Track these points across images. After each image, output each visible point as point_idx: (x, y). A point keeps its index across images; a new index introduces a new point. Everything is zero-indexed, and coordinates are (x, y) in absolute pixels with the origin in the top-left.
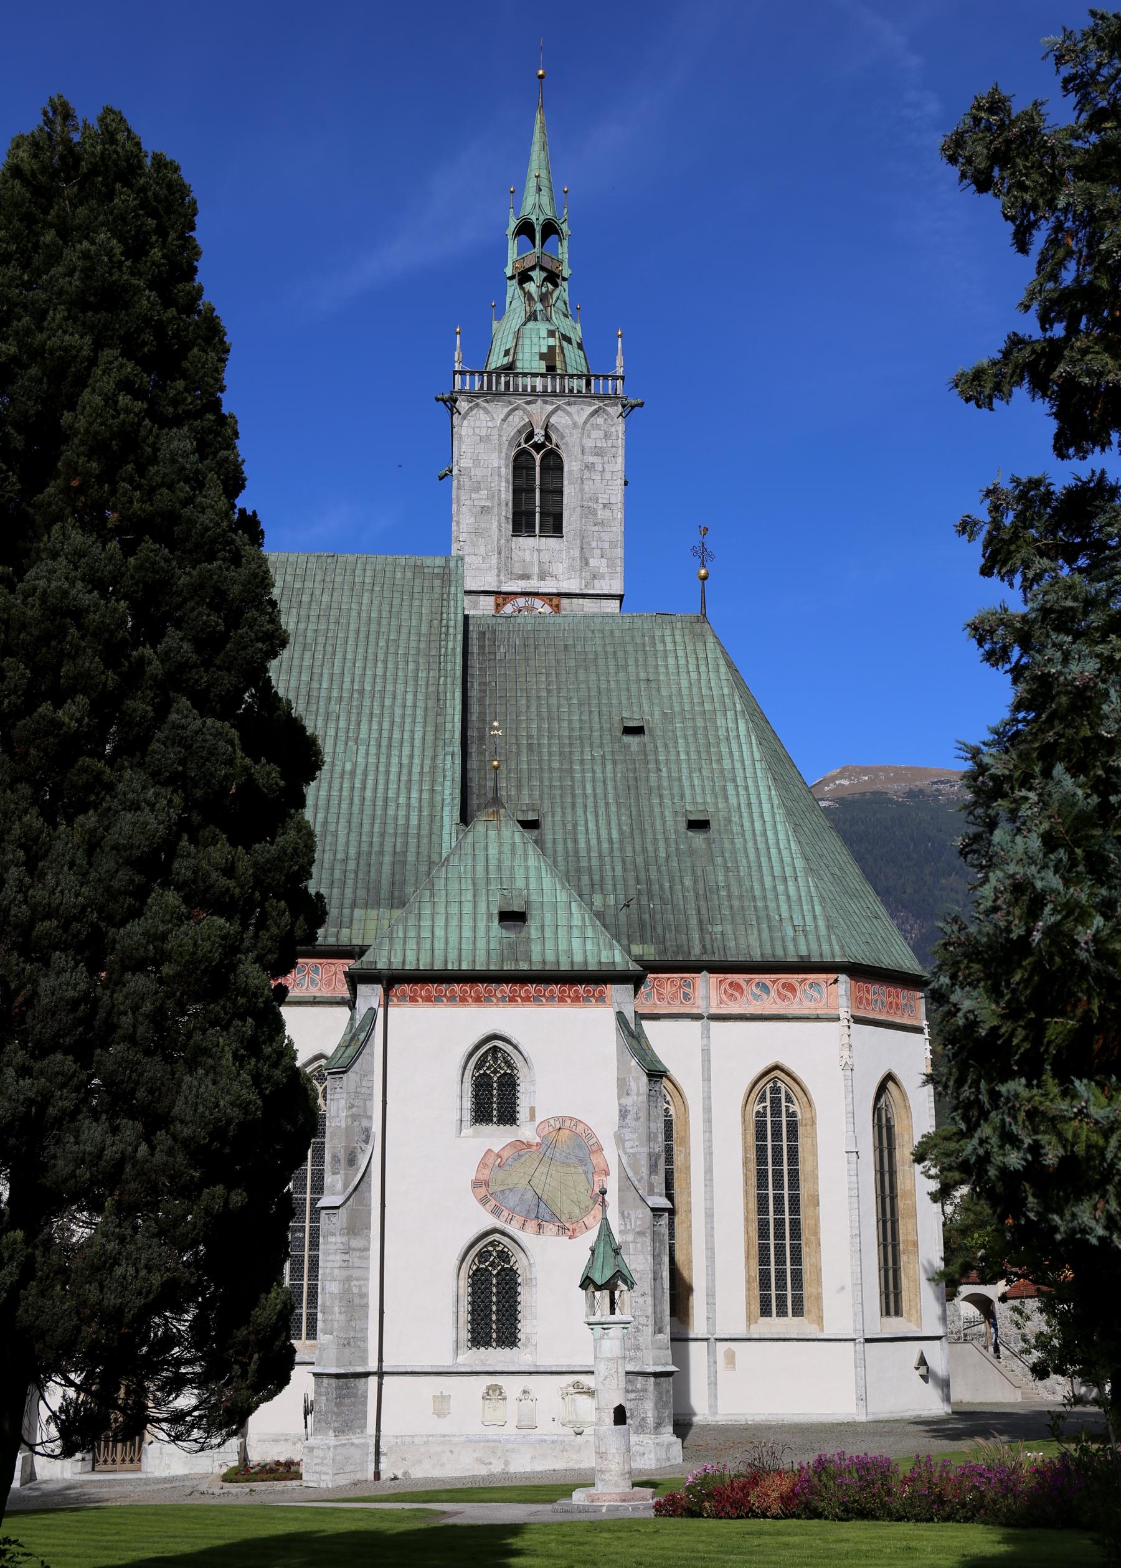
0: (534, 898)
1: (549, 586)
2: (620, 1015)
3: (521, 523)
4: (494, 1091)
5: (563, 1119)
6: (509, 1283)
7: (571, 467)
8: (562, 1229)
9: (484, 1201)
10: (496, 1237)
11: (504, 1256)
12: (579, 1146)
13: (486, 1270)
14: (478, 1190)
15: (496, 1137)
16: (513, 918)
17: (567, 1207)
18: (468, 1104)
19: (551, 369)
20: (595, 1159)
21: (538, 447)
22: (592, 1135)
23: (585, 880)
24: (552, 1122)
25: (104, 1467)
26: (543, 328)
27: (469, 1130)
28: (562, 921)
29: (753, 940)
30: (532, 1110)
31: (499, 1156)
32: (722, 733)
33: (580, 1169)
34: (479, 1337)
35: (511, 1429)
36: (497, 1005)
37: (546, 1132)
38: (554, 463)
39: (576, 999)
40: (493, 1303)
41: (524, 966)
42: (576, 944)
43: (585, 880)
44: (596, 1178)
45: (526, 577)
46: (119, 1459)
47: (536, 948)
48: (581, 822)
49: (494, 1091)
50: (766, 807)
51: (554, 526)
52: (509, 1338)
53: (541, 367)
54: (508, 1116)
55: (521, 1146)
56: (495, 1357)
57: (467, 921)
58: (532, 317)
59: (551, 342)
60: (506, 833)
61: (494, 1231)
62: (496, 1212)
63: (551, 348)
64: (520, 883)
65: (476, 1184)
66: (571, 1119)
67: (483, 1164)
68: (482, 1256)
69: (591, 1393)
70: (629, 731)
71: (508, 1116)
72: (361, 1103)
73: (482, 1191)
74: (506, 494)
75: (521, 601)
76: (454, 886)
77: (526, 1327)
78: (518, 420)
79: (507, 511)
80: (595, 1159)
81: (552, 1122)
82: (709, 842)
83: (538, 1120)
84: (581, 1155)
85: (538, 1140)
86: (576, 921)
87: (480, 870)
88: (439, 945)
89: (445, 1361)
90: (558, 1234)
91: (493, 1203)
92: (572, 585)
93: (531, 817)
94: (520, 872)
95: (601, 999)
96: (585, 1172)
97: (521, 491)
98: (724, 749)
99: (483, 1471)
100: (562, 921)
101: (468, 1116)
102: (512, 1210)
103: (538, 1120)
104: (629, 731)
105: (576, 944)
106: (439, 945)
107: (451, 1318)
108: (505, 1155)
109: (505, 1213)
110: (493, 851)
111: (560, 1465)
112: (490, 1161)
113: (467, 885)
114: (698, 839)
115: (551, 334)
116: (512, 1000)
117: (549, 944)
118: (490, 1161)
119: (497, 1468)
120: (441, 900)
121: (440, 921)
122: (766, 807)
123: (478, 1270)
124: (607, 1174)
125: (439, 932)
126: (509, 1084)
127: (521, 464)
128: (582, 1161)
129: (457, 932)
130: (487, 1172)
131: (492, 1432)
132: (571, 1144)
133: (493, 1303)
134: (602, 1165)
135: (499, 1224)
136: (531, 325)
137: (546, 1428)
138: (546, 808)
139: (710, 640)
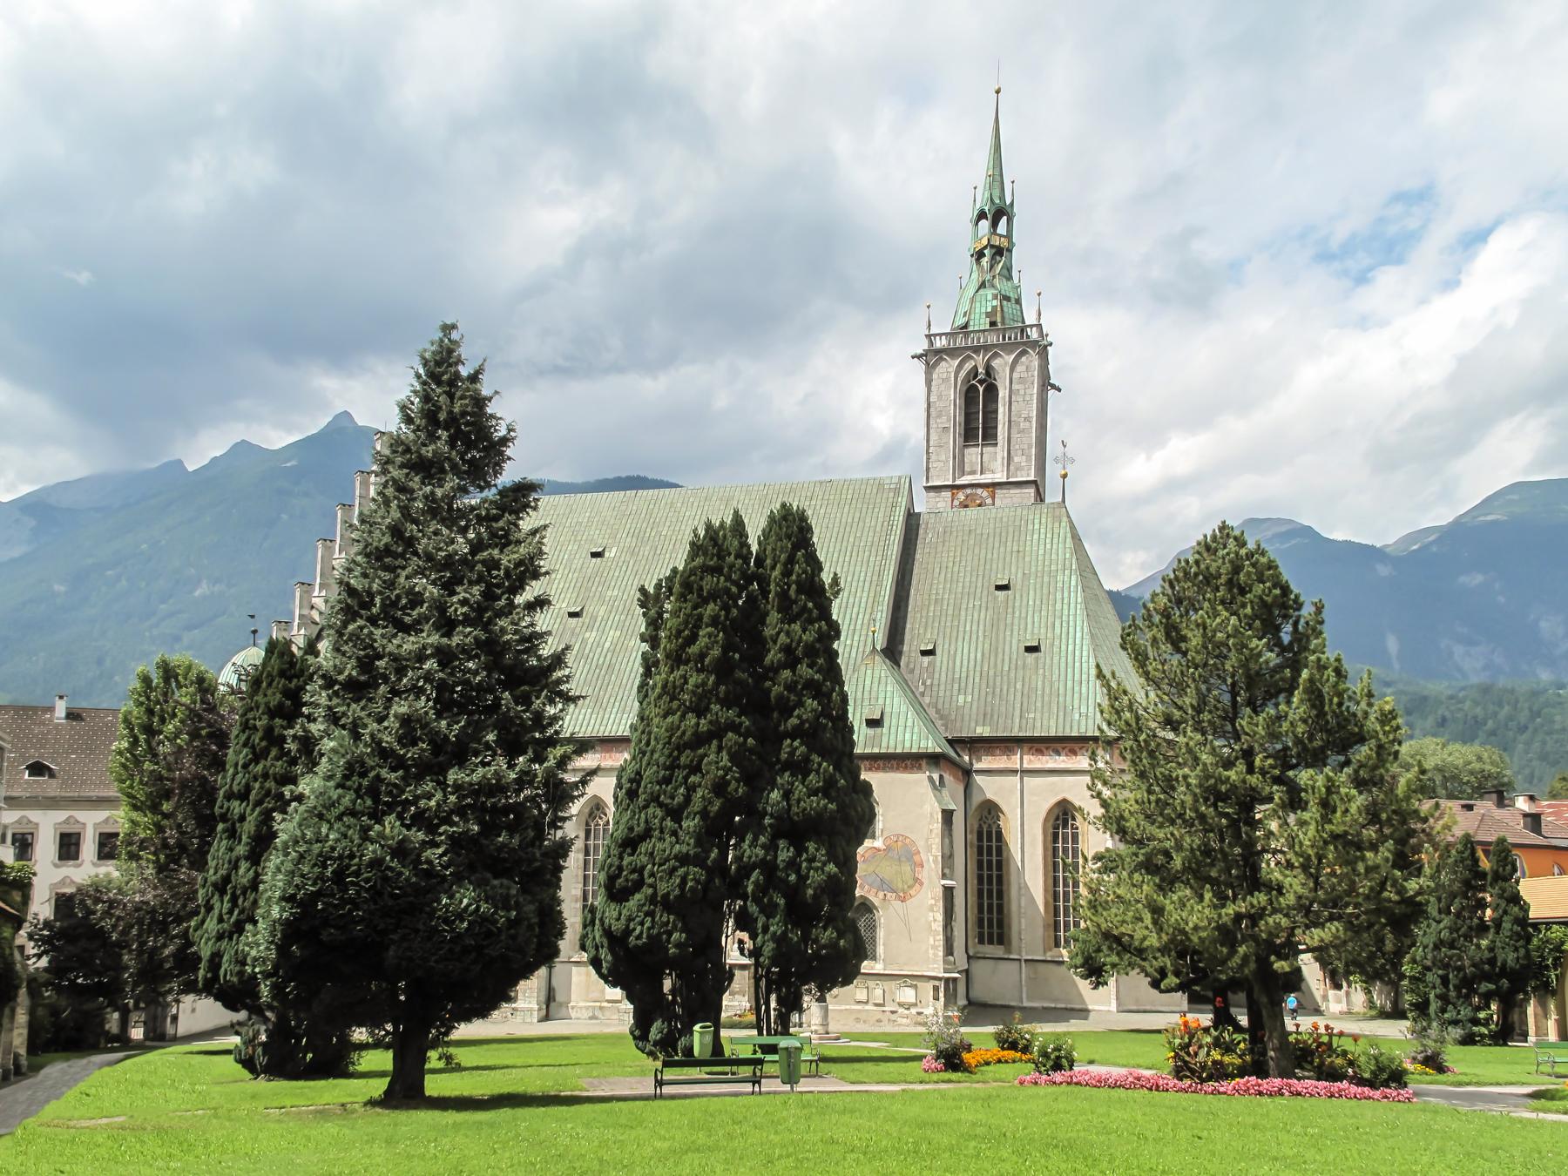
1: (987, 478)
3: (969, 435)
7: (1003, 393)
19: (993, 324)
21: (981, 382)
23: (956, 686)
26: (989, 293)
28: (902, 722)
29: (1053, 723)
32: (1060, 585)
38: (992, 391)
41: (876, 750)
43: (956, 686)
45: (973, 472)
50: (1079, 635)
51: (990, 435)
53: (984, 324)
58: (982, 285)
59: (994, 303)
63: (994, 308)
64: (881, 701)
70: (999, 588)
74: (960, 418)
75: (969, 491)
78: (968, 366)
79: (960, 429)
80: (916, 858)
82: (1037, 659)
86: (909, 723)
92: (1000, 477)
93: (930, 647)
94: (882, 695)
97: (969, 417)
98: (1059, 596)
100: (902, 722)
104: (999, 588)
110: (868, 682)
114: (1031, 657)
115: (995, 297)
117: (893, 737)
122: (1079, 635)
127: (969, 395)
136: (982, 292)
138: (940, 642)
139: (1065, 519)
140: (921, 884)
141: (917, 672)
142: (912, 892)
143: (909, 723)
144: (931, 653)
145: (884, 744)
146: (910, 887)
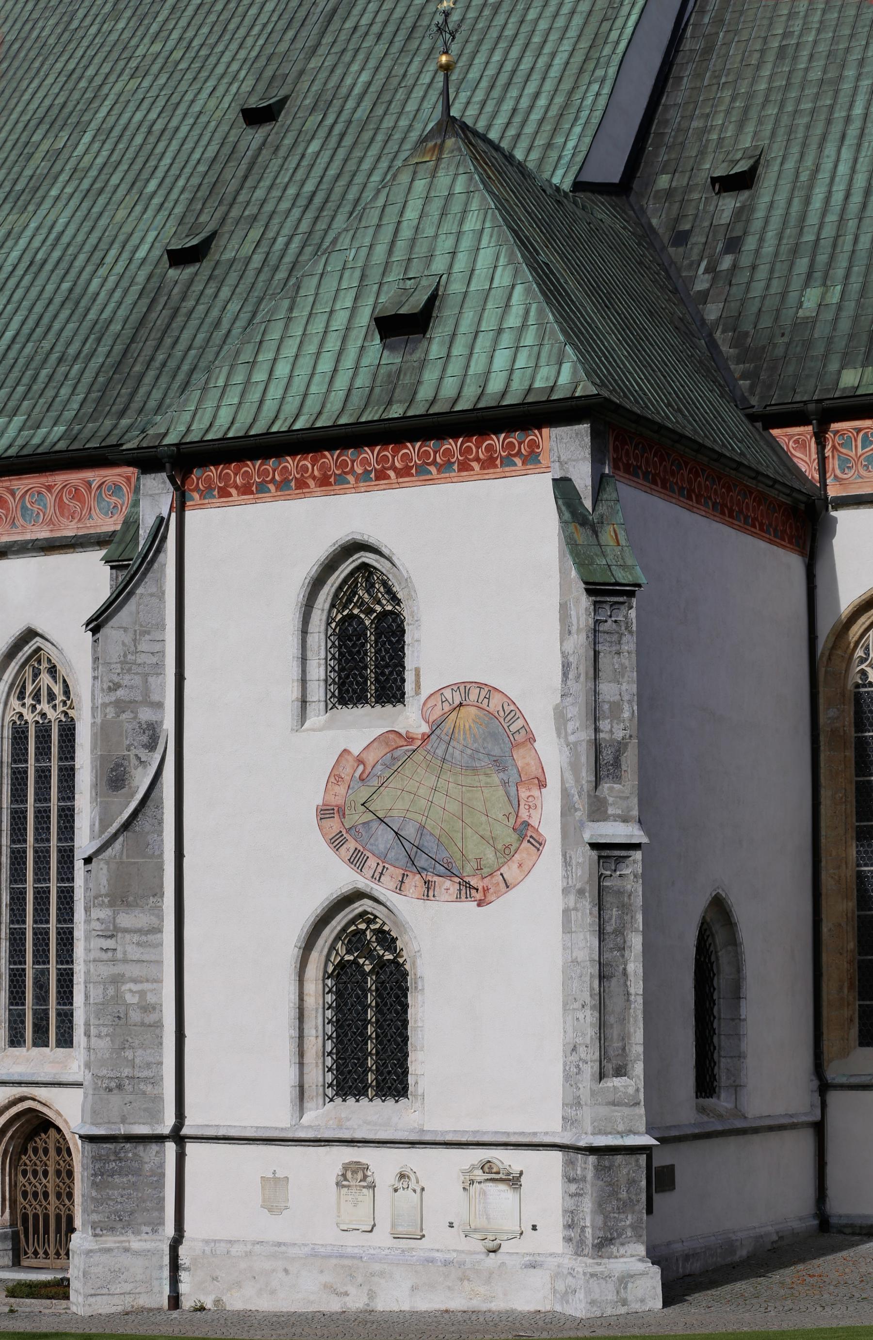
0: (456, 287)
2: (563, 488)
4: (363, 642)
5: (464, 687)
6: (395, 984)
8: (466, 889)
9: (336, 842)
10: (365, 905)
11: (387, 939)
12: (494, 736)
13: (355, 962)
14: (327, 823)
15: (362, 728)
16: (403, 327)
17: (474, 848)
18: (317, 671)
20: (521, 758)
22: (514, 713)
23: (802, 265)
24: (448, 693)
25: (33, 1262)
27: (317, 717)
28: (489, 323)
30: (417, 672)
31: (360, 761)
33: (496, 779)
34: (348, 1082)
35: (382, 1238)
36: (356, 489)
37: (437, 713)
39: (489, 463)
40: (366, 1022)
41: (396, 411)
42: (501, 360)
43: (802, 265)
44: (523, 794)
46: (52, 1251)
47: (430, 376)
48: (827, 165)
49: (363, 642)
52: (394, 1083)
54: (391, 691)
55: (398, 743)
56: (368, 1115)
57: (333, 343)
60: (443, 180)
61: (357, 895)
62: (357, 861)
64: (439, 265)
65: (325, 813)
66: (480, 686)
67: (335, 777)
68: (354, 939)
69: (514, 1181)
71: (391, 691)
72: (137, 680)
73: (334, 825)
76: (330, 284)
77: (423, 1064)
80: (521, 758)
81: (448, 693)
83: (425, 692)
84: (496, 751)
85: (425, 729)
86: (513, 320)
87: (380, 250)
88: (275, 392)
89: (279, 1117)
90: (459, 898)
91: (352, 845)
94: (445, 244)
95: (532, 458)
96: (505, 784)
99: (334, 1305)
100: (489, 323)
101: (317, 692)
102: (383, 857)
103: (425, 692)
105: (501, 360)
106: (275, 392)
107: (286, 1048)
108: (371, 758)
109: (372, 862)
110: (411, 214)
111: (457, 1303)
112: (346, 772)
113: (351, 280)
116: (381, 475)
117: (455, 368)
118: (346, 772)
119: (356, 1302)
120: (301, 314)
121: (289, 350)
123: (342, 966)
124: (542, 784)
125: (282, 370)
126: (392, 631)
128: (499, 764)
129: (319, 363)
130: (341, 790)
131: (353, 1242)
132: (486, 732)
133: (366, 1022)
134: (534, 771)
135: (362, 883)
137: (440, 1240)
138: (776, 151)
140: (538, 844)
141: (697, 239)
142: (510, 871)
143: (513, 320)
144: (741, 182)
145: (425, 393)
146: (507, 853)
